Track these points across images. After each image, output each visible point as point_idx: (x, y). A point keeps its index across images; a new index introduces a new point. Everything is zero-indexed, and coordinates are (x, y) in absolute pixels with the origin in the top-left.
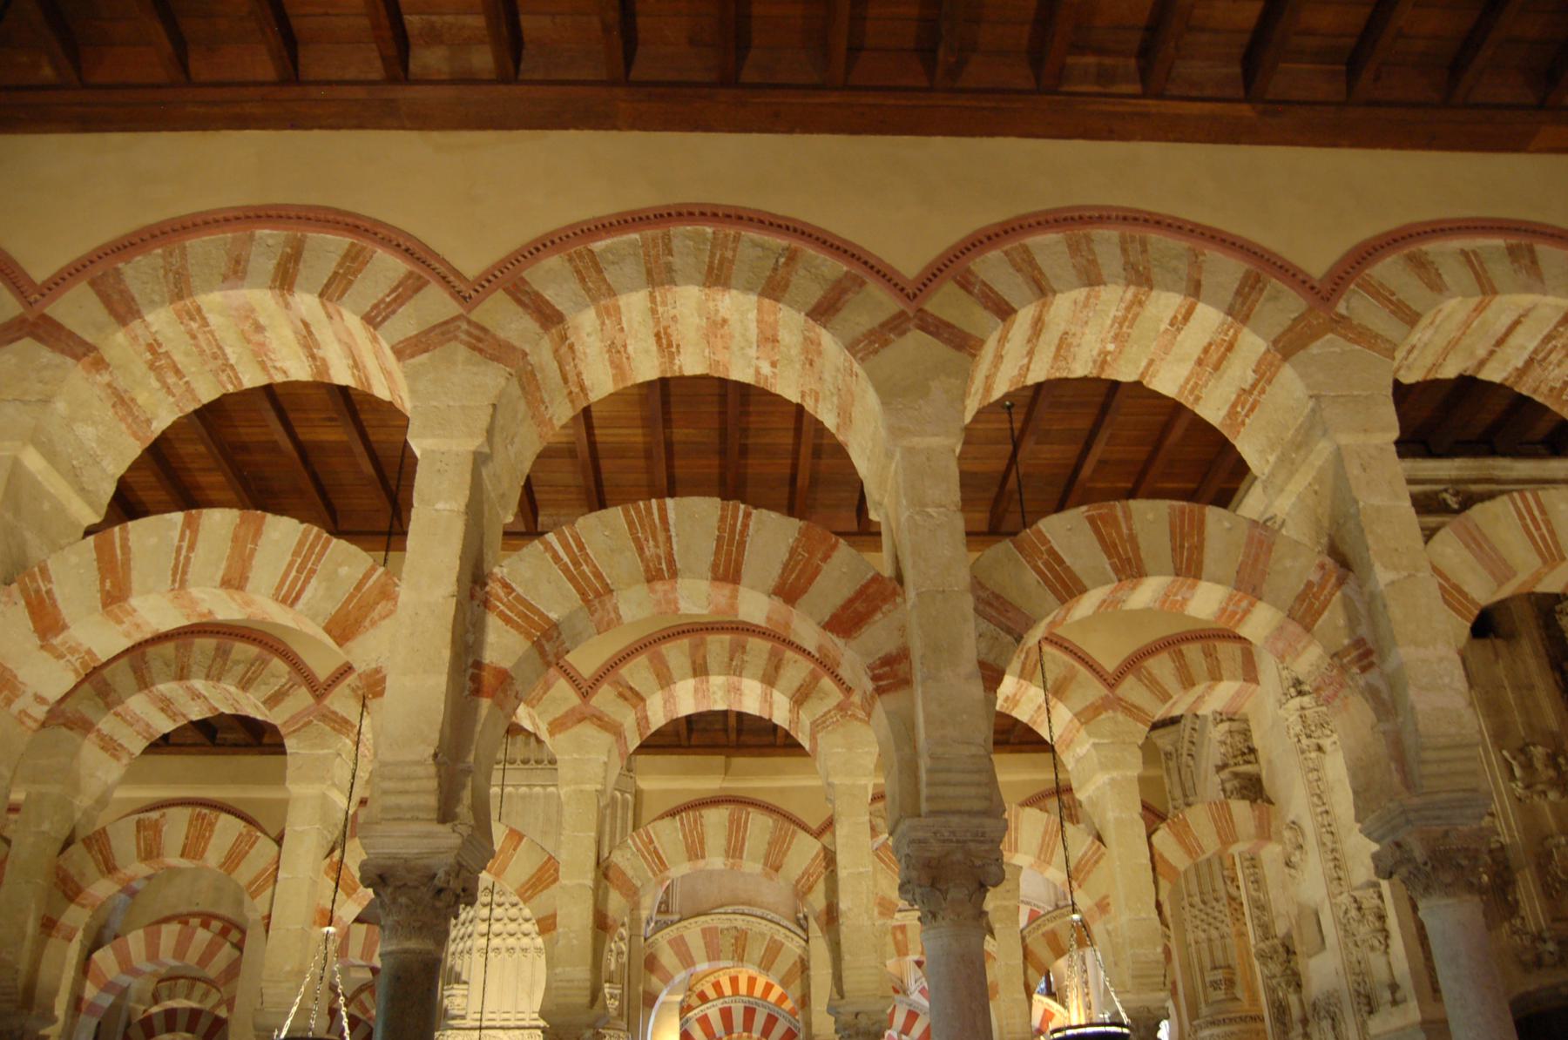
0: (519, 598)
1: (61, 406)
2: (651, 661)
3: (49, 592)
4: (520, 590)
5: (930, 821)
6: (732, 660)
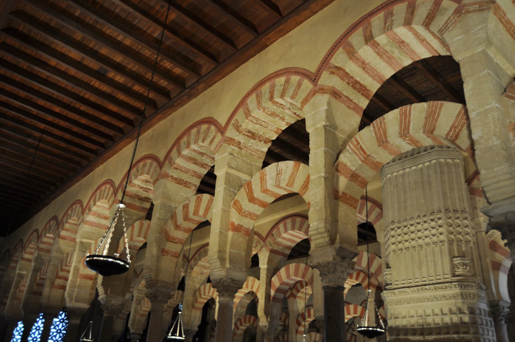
2: (344, 48)
6: (385, 24)
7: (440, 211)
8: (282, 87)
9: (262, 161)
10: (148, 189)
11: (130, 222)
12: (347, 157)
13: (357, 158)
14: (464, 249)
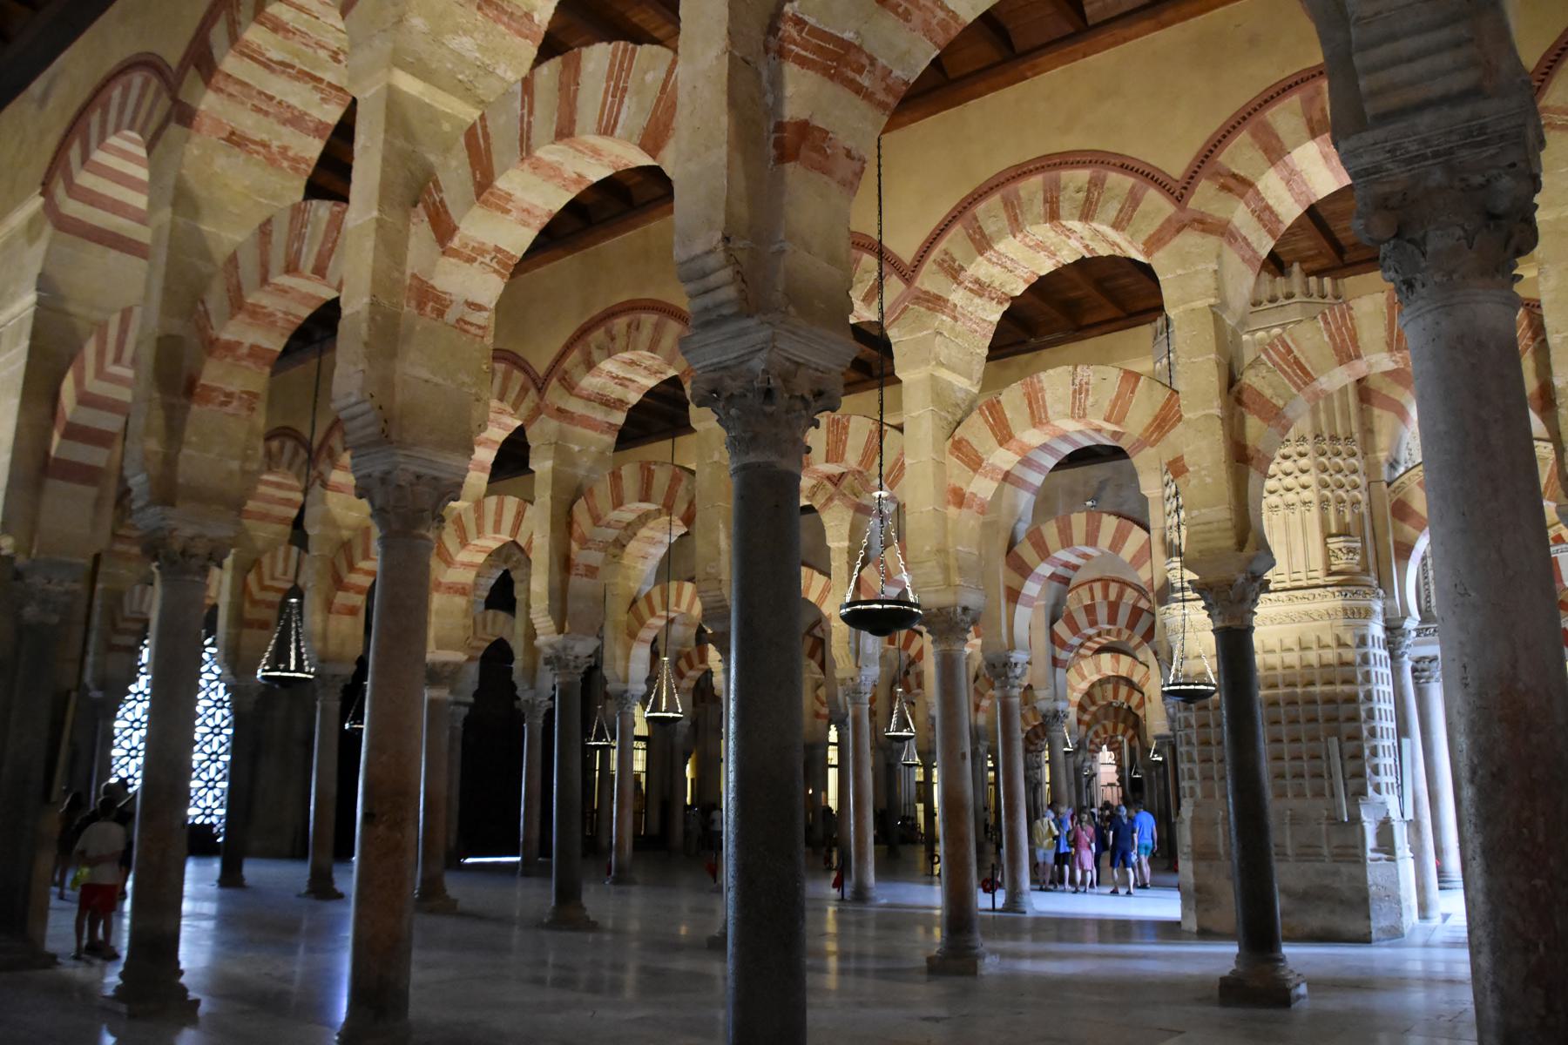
0: (815, 32)
1: (417, 22)
2: (1254, 135)
3: (441, 201)
4: (812, 21)
5: (1379, 133)
7: (1304, 439)
8: (1082, 195)
9: (988, 343)
10: (626, 379)
12: (1263, 378)
13: (1287, 381)
14: (1348, 518)
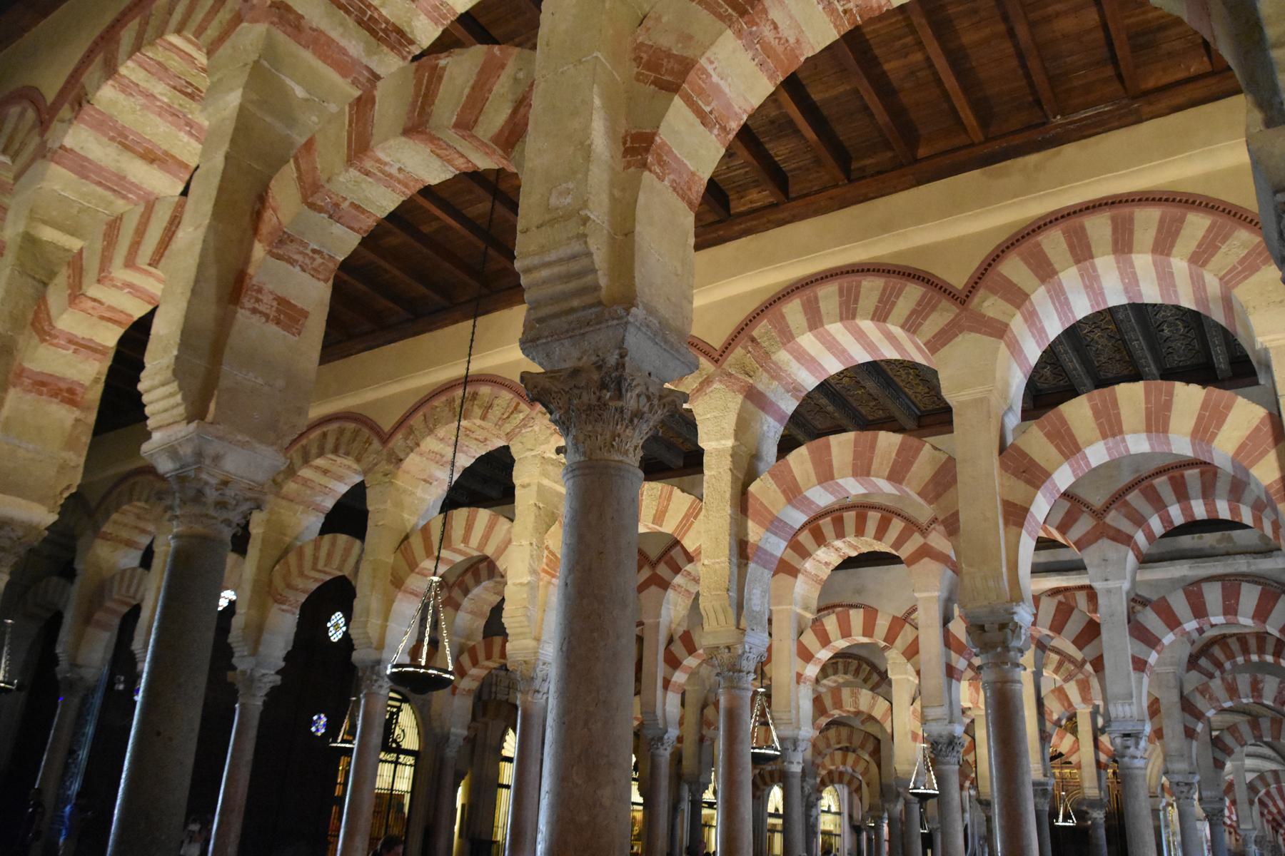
11: (314, 119)
